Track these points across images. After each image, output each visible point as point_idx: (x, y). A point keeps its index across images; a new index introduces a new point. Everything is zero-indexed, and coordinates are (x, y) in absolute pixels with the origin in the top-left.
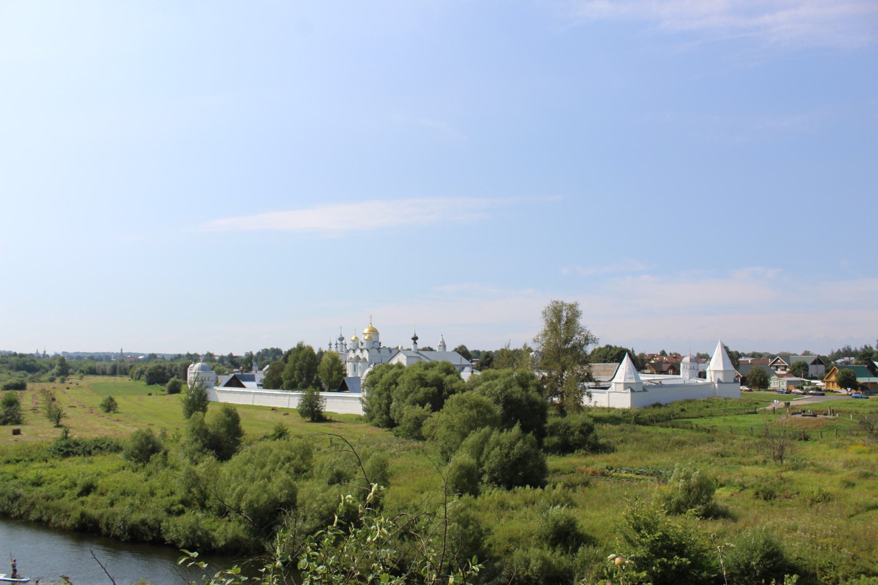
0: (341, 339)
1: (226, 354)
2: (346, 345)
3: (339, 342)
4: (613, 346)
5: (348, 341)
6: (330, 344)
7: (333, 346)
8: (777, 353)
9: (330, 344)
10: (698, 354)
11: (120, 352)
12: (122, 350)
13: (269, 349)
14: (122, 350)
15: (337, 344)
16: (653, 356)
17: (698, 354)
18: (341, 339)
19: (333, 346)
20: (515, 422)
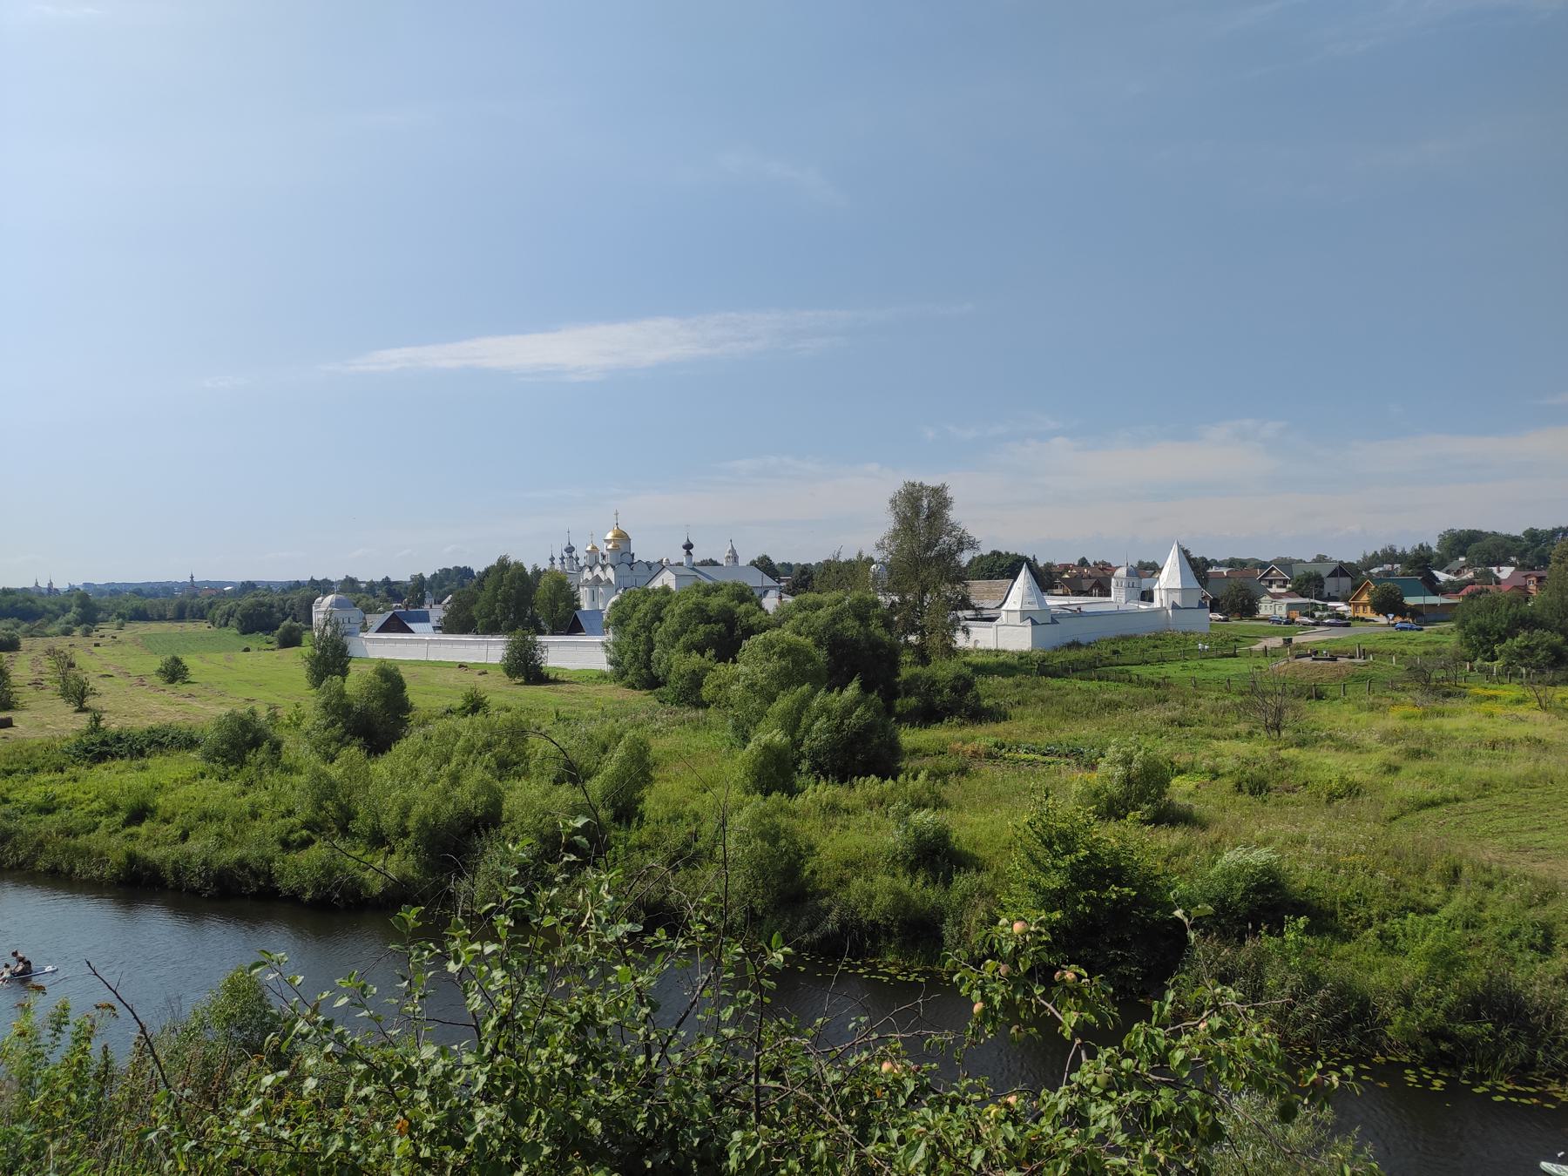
0: (570, 550)
2: (577, 559)
3: (566, 555)
5: (581, 553)
6: (552, 559)
7: (557, 561)
9: (552, 559)
10: (1140, 563)
11: (189, 580)
12: (192, 577)
14: (192, 577)
15: (562, 558)
16: (1066, 568)
17: (1140, 563)
18: (570, 550)
19: (557, 561)
20: (850, 680)
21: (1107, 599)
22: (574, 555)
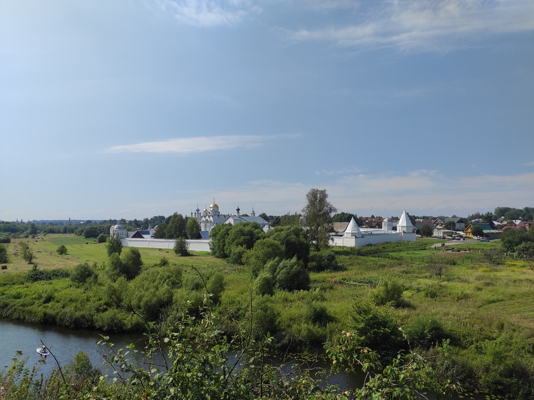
0: (198, 210)
1: (133, 220)
2: (200, 213)
3: (196, 212)
4: (346, 213)
5: (202, 212)
6: (192, 213)
7: (194, 214)
9: (192, 213)
10: (392, 217)
11: (69, 220)
12: (70, 219)
13: (5, 221)
14: (70, 219)
15: (195, 213)
16: (367, 218)
17: (392, 217)
18: (198, 210)
19: (194, 214)
21: (381, 229)
22: (199, 212)
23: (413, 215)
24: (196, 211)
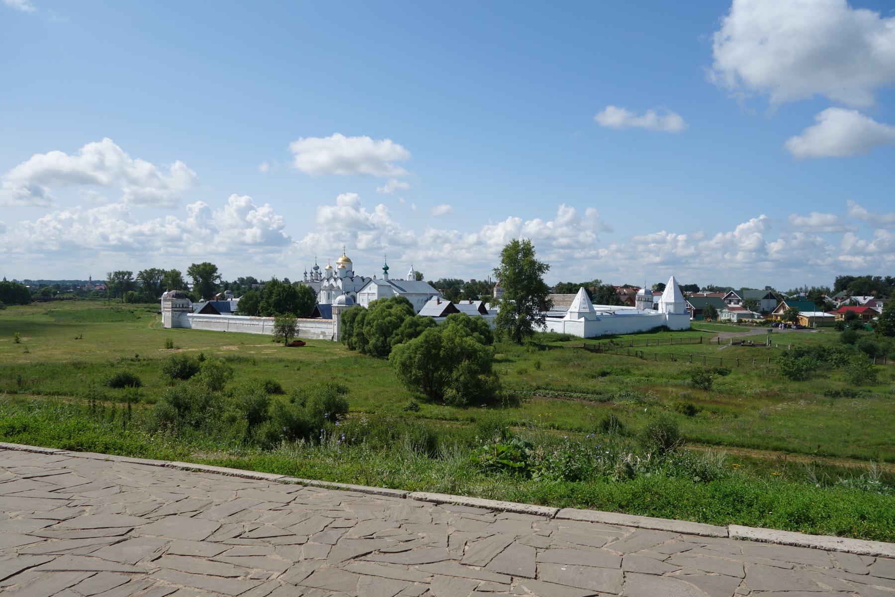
0: (317, 268)
3: (314, 271)
6: (305, 273)
7: (309, 275)
8: (583, 282)
9: (305, 273)
10: (163, 270)
11: (88, 279)
12: (90, 278)
14: (90, 278)
15: (312, 273)
17: (163, 270)
18: (317, 268)
19: (309, 275)
21: (330, 320)
23: (209, 262)
24: (314, 268)
